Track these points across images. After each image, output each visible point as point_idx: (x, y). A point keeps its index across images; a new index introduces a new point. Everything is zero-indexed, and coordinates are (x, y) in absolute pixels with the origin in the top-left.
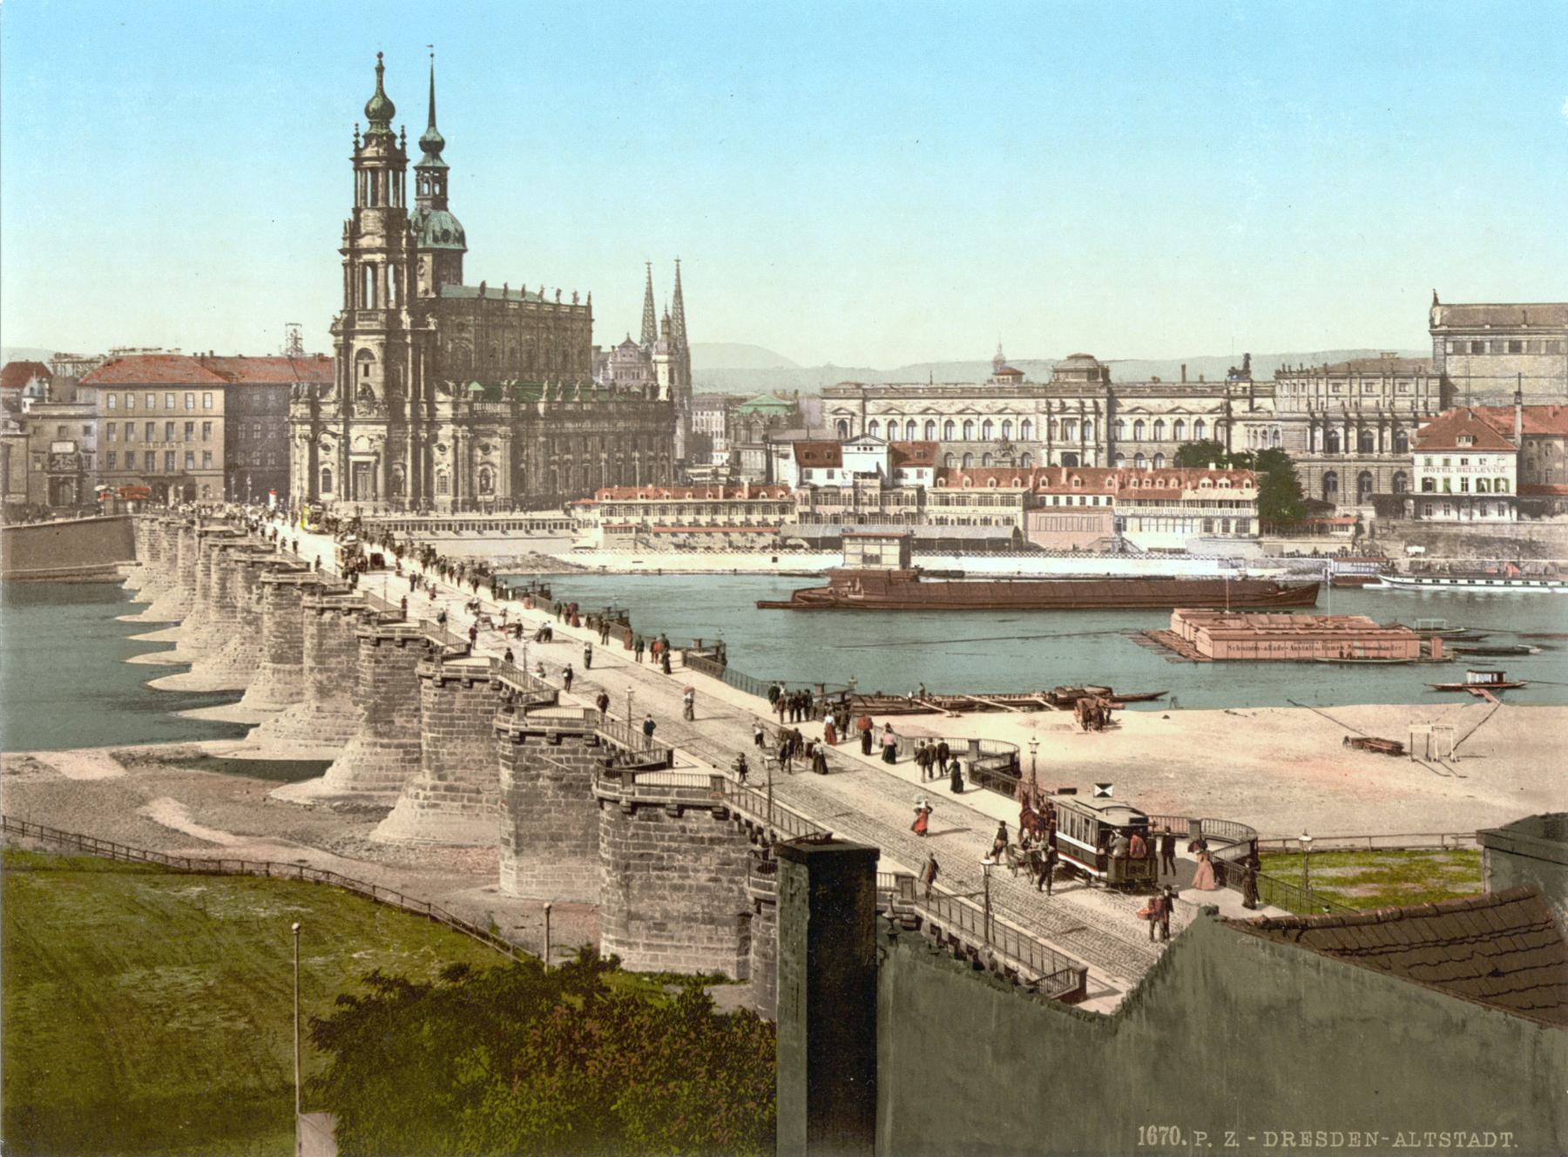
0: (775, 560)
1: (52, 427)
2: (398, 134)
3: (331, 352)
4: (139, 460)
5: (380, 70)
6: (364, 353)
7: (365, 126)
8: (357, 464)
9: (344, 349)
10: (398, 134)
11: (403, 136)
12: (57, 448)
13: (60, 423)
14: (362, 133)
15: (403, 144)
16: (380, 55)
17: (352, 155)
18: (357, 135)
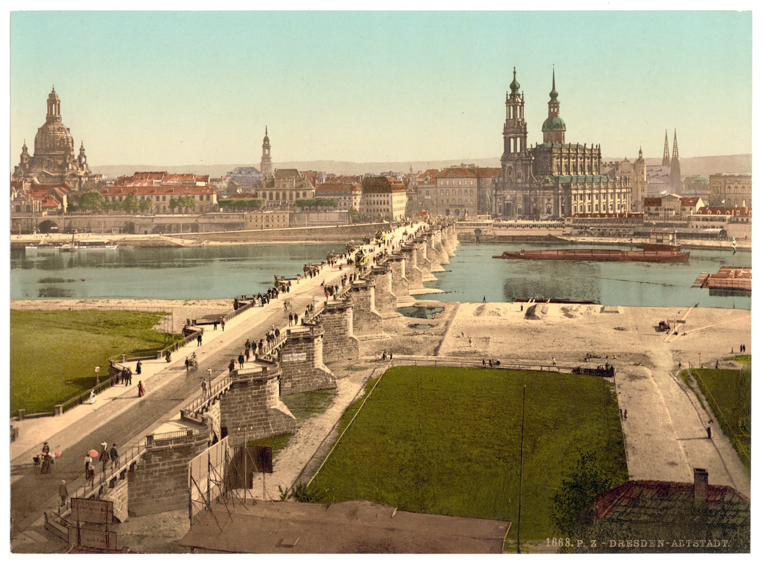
0: (530, 314)
1: (424, 191)
2: (521, 94)
3: (501, 167)
4: (445, 201)
5: (515, 73)
6: (510, 167)
7: (510, 92)
8: (507, 204)
9: (504, 166)
10: (521, 94)
12: (426, 197)
13: (427, 189)
14: (509, 94)
16: (514, 68)
17: (505, 101)
18: (507, 95)
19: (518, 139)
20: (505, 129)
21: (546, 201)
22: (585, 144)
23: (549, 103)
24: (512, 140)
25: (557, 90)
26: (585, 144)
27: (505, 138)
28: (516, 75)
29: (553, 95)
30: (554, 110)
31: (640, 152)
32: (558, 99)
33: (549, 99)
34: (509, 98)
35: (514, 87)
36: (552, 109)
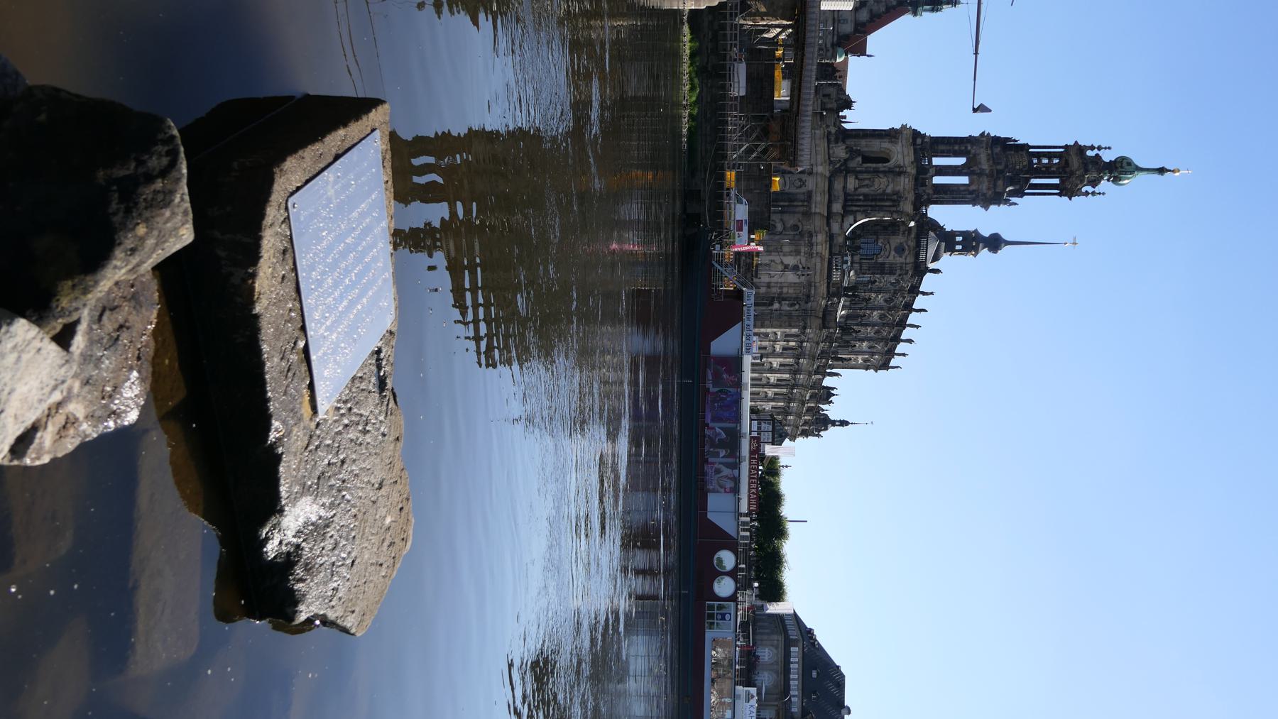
2: (1097, 190)
5: (1162, 171)
7: (1107, 157)
11: (1093, 193)
14: (1101, 153)
15: (1087, 194)
17: (1081, 143)
18: (1099, 148)
19: (964, 180)
20: (997, 140)
21: (790, 261)
22: (910, 341)
23: (976, 231)
24: (961, 161)
25: (1006, 250)
26: (910, 341)
27: (970, 140)
28: (1156, 176)
29: (995, 243)
30: (959, 243)
31: (844, 423)
32: (985, 253)
33: (986, 233)
34: (1090, 153)
35: (1120, 169)
36: (959, 239)
